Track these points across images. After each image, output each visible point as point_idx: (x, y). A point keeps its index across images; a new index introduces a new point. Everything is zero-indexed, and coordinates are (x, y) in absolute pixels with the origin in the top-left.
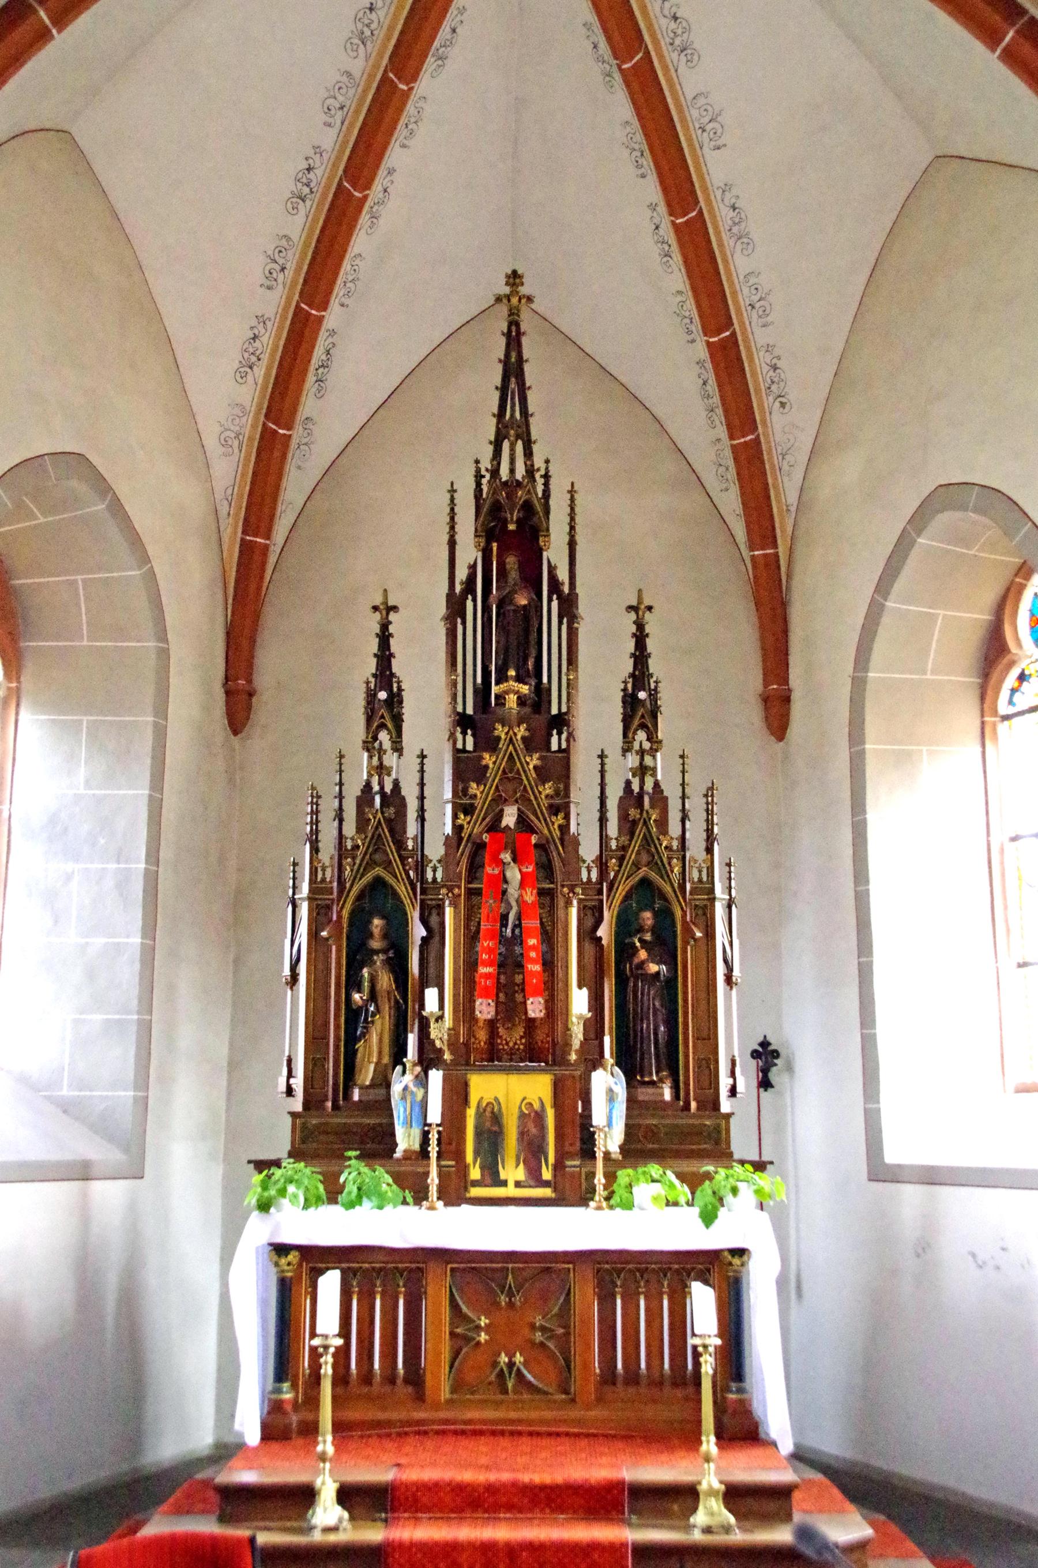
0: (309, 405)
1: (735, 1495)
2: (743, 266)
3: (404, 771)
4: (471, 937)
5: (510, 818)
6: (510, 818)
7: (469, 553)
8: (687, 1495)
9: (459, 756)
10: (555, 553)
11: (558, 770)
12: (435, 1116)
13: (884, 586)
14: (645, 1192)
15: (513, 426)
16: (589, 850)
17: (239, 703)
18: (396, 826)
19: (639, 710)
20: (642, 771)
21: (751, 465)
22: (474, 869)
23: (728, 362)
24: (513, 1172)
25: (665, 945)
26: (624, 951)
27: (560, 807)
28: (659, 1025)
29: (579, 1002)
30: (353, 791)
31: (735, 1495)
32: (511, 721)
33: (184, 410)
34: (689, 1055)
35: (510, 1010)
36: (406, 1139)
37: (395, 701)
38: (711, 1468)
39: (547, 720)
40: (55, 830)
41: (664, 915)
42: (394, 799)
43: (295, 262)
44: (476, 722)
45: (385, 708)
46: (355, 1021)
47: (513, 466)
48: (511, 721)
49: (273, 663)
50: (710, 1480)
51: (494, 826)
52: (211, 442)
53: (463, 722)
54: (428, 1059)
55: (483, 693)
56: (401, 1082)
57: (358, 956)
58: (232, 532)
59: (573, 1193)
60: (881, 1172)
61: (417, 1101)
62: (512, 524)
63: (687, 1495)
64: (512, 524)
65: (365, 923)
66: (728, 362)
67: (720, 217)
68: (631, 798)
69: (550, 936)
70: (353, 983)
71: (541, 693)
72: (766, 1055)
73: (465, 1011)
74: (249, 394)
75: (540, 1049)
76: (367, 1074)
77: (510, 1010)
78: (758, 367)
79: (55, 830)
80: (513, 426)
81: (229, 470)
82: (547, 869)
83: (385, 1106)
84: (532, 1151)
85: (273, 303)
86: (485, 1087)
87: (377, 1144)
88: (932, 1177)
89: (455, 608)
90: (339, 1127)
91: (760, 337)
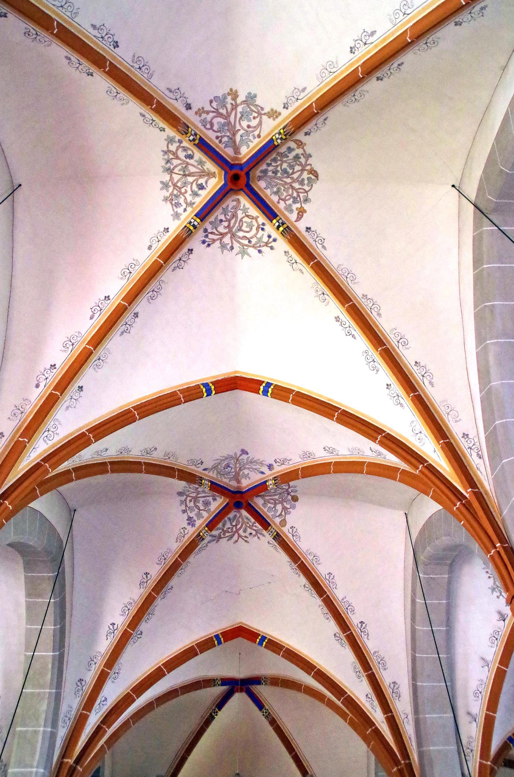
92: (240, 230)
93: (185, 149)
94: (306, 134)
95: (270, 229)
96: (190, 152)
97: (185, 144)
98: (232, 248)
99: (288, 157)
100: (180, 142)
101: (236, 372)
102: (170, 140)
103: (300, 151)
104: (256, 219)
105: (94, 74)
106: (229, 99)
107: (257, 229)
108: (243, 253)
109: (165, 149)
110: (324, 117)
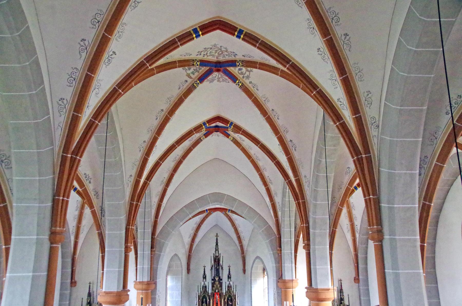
2: (239, 229)
3: (206, 283)
5: (217, 291)
6: (217, 291)
7: (213, 262)
9: (212, 283)
10: (221, 262)
11: (221, 286)
13: (253, 264)
15: (217, 249)
16: (224, 292)
19: (229, 277)
20: (229, 284)
21: (242, 247)
22: (214, 296)
23: (239, 238)
25: (231, 301)
26: (228, 302)
27: (221, 290)
30: (202, 286)
32: (217, 280)
33: (183, 242)
39: (220, 279)
43: (195, 229)
44: (214, 280)
45: (205, 277)
48: (217, 280)
49: (192, 267)
51: (215, 292)
52: (185, 244)
53: (212, 280)
55: (214, 277)
57: (203, 302)
58: (188, 253)
62: (217, 260)
64: (217, 260)
66: (239, 238)
67: (237, 226)
68: (228, 287)
69: (221, 302)
71: (220, 278)
74: (190, 240)
78: (242, 237)
80: (217, 249)
81: (187, 247)
89: (212, 269)
91: (242, 235)
92: (216, 50)
93: (242, 73)
94: (186, 81)
95: (201, 57)
96: (240, 72)
97: (241, 76)
98: (221, 47)
99: (194, 69)
100: (243, 77)
101: (219, 17)
102: (248, 77)
103: (189, 72)
104: (208, 56)
106: (221, 80)
107: (207, 54)
108: (215, 45)
109: (251, 73)
110: (180, 90)
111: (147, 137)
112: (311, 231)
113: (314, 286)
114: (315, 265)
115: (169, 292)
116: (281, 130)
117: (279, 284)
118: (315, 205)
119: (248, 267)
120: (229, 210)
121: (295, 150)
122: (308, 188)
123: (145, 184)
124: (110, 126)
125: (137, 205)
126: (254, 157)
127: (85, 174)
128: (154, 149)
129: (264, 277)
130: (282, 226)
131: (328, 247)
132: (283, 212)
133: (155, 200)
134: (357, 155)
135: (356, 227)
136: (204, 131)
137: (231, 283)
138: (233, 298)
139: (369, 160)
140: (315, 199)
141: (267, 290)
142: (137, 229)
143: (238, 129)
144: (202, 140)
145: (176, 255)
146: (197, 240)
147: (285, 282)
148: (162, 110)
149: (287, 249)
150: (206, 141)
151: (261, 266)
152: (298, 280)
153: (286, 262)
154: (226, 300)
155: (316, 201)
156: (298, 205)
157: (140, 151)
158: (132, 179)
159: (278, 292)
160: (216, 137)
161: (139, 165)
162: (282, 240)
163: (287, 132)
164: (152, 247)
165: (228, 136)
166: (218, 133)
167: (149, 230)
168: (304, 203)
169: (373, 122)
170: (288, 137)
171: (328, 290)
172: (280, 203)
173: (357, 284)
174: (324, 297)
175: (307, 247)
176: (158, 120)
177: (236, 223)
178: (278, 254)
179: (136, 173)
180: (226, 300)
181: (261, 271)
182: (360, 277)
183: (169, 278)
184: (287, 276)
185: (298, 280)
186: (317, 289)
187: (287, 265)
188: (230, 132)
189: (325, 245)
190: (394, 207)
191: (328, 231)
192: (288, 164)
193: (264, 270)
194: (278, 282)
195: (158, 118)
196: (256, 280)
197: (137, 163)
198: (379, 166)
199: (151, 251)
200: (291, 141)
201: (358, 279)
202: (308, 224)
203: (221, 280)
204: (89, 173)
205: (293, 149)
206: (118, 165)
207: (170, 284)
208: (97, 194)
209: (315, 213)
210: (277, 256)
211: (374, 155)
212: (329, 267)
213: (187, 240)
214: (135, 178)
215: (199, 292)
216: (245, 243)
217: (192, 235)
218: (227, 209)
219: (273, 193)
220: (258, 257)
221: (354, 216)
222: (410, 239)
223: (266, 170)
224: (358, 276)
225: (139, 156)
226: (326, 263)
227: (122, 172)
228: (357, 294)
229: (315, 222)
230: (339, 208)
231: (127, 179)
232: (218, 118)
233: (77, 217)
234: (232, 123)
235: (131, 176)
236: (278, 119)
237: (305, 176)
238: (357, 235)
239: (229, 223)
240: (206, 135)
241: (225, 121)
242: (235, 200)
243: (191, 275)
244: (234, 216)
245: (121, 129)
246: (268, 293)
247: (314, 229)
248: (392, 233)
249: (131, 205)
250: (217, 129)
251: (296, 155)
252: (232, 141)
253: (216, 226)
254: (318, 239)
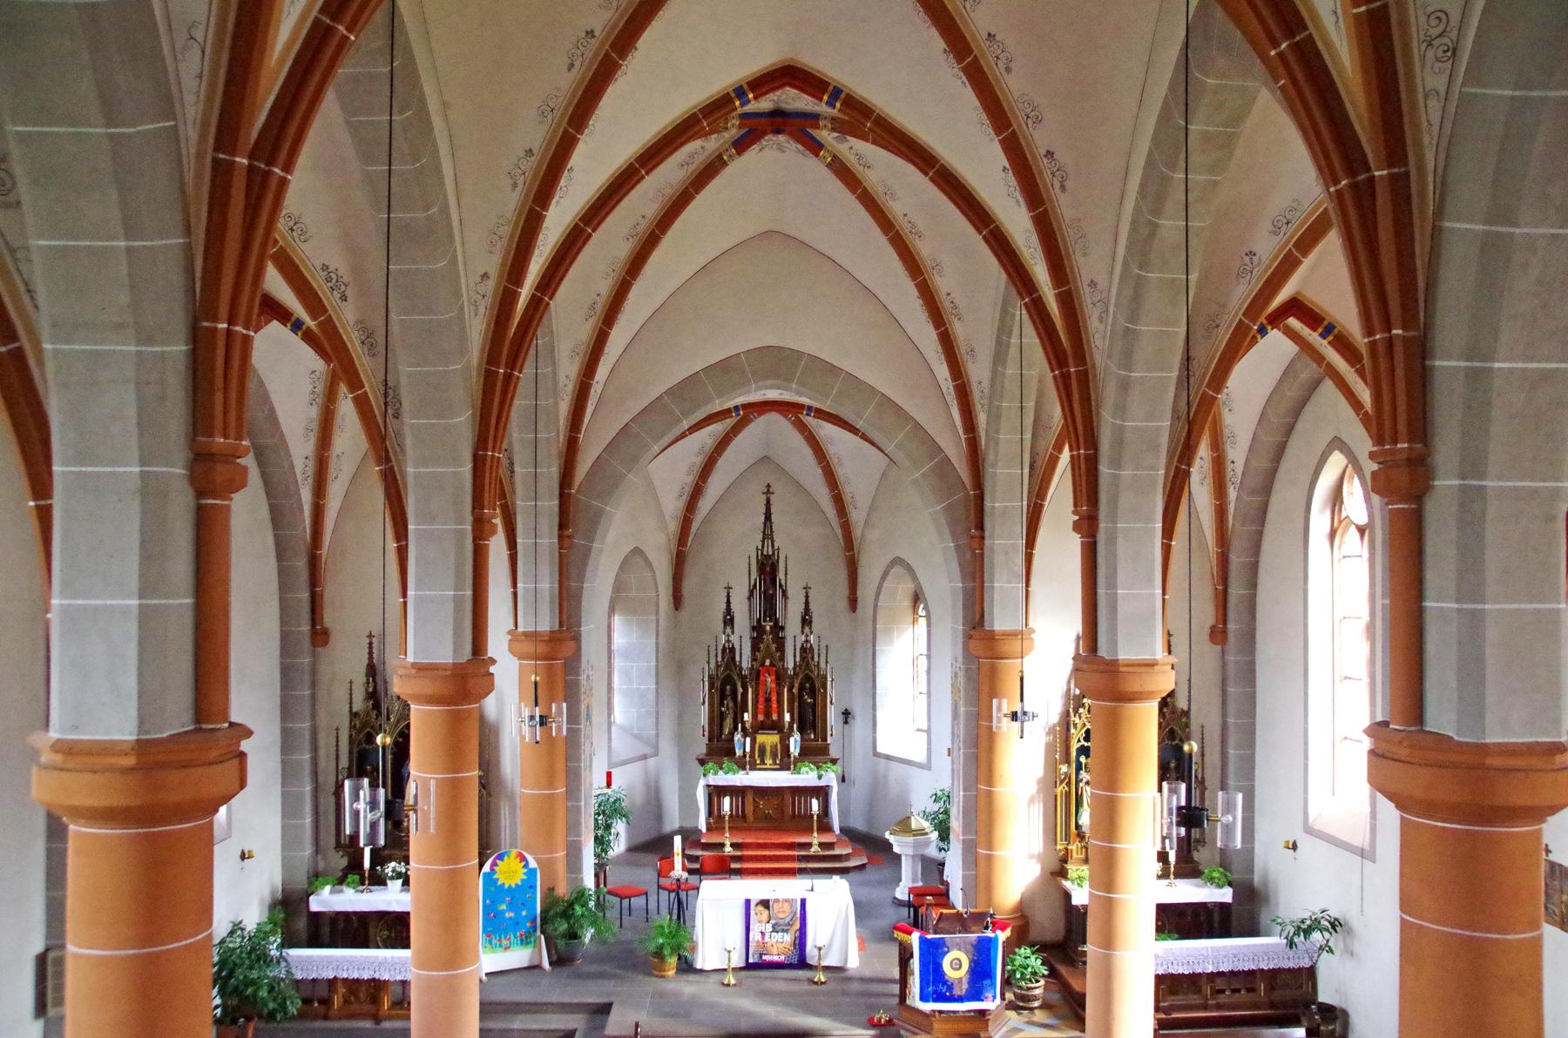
0: (700, 504)
1: (821, 845)
2: (841, 472)
3: (734, 639)
4: (756, 695)
5: (768, 663)
6: (768, 663)
7: (754, 575)
8: (810, 845)
9: (753, 639)
10: (781, 575)
11: (781, 648)
12: (748, 749)
13: (883, 578)
14: (804, 769)
16: (790, 665)
17: (677, 600)
18: (733, 658)
19: (806, 621)
22: (758, 678)
23: (839, 501)
24: (769, 761)
25: (813, 693)
26: (801, 695)
27: (782, 659)
28: (810, 721)
29: (787, 717)
30: (720, 648)
31: (821, 845)
32: (768, 631)
34: (819, 725)
35: (768, 714)
36: (739, 752)
37: (732, 620)
38: (816, 839)
39: (778, 628)
40: (627, 654)
41: (813, 685)
42: (732, 650)
43: (697, 469)
44: (757, 628)
45: (729, 620)
46: (722, 717)
47: (768, 551)
48: (768, 631)
49: (689, 585)
50: (815, 842)
51: (763, 665)
53: (754, 628)
54: (744, 729)
55: (759, 621)
56: (738, 737)
57: (723, 697)
59: (784, 767)
60: (876, 754)
61: (742, 744)
62: (768, 568)
63: (810, 845)
64: (768, 568)
65: (726, 688)
66: (839, 501)
67: (834, 461)
68: (803, 649)
69: (780, 695)
70: (722, 704)
71: (776, 622)
72: (847, 714)
73: (755, 716)
75: (777, 727)
76: (726, 731)
77: (768, 714)
78: (847, 499)
79: (627, 654)
81: (673, 527)
82: (778, 678)
83: (732, 740)
84: (774, 756)
85: (690, 480)
86: (760, 738)
87: (730, 752)
88: (888, 757)
90: (719, 750)
91: (848, 490)
105: (985, 36)
111: (535, 135)
112: (1104, 469)
113: (1103, 651)
114: (1112, 585)
115: (618, 663)
116: (1018, 112)
117: (972, 644)
118: (1125, 386)
119: (866, 592)
120: (810, 408)
121: (1063, 187)
122: (1101, 327)
123: (537, 305)
124: (400, 85)
125: (508, 378)
126: (903, 225)
127: (325, 267)
128: (563, 182)
129: (914, 621)
130: (990, 458)
131: (1159, 525)
132: (995, 416)
133: (568, 370)
134: (1351, 171)
135: (1229, 467)
136: (733, 131)
137: (812, 638)
138: (817, 684)
139: (1401, 188)
140: (1127, 361)
141: (923, 661)
142: (512, 464)
143: (859, 117)
144: (725, 164)
145: (637, 551)
146: (705, 505)
147: (991, 638)
148: (590, 34)
149: (1004, 537)
150: (742, 167)
151: (907, 587)
152: (1033, 631)
153: (997, 576)
154: (795, 691)
155: (1129, 368)
156: (1063, 383)
157: (515, 185)
158: (490, 286)
159: (967, 670)
160: (775, 158)
161: (512, 237)
162: (988, 504)
163: (1038, 121)
164: (563, 526)
165: (815, 147)
166: (782, 138)
167: (551, 471)
168: (1085, 379)
169: (1435, 32)
170: (1039, 140)
171: (1151, 664)
172: (986, 384)
173: (1219, 647)
174: (1136, 688)
175: (1088, 525)
176: (575, 71)
177: (832, 451)
178: (973, 550)
179: (503, 265)
180: (795, 691)
181: (907, 603)
182: (1231, 626)
183: (617, 621)
184: (1001, 620)
185: (1033, 631)
186: (1114, 663)
187: (1003, 583)
188: (825, 135)
189: (1151, 520)
190: (1491, 370)
191: (1162, 472)
192: (1035, 240)
193: (917, 598)
194: (968, 637)
195: (577, 64)
196: (889, 631)
197: (506, 231)
198: (1439, 213)
199: (561, 537)
200: (1050, 154)
201: (1224, 632)
202: (1096, 449)
203: (782, 628)
204: (339, 264)
205: (1057, 185)
206: (436, 235)
207: (619, 640)
208: (368, 338)
209: (1121, 410)
210: (968, 555)
211: (1421, 168)
212: (1159, 591)
213: (673, 505)
214: (499, 283)
215: (713, 665)
216: (857, 516)
217: (688, 489)
218: (801, 407)
219: (962, 347)
220: (897, 561)
221: (1226, 431)
222: (1536, 491)
223: (939, 272)
224: (1225, 623)
225: (510, 202)
226: (1151, 580)
227: (455, 257)
228: (1216, 678)
229: (1119, 441)
230: (1204, 395)
231: (472, 285)
232: (789, 74)
233: (315, 426)
234: (837, 92)
235: (485, 276)
236: (1008, 70)
237: (1093, 284)
238: (1232, 494)
239: (807, 452)
240: (741, 145)
241: (811, 83)
242: (833, 370)
243: (685, 613)
244: (826, 431)
245: (445, 105)
246: (929, 672)
247: (1117, 463)
248: (1473, 465)
249: (489, 378)
250: (780, 121)
251: (1065, 207)
252: (829, 166)
253: (765, 459)
254: (1126, 500)
